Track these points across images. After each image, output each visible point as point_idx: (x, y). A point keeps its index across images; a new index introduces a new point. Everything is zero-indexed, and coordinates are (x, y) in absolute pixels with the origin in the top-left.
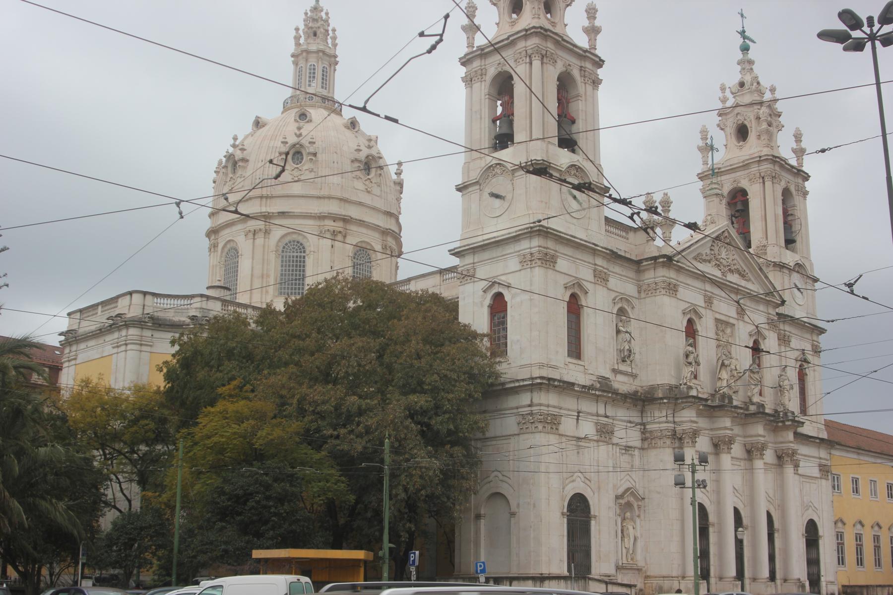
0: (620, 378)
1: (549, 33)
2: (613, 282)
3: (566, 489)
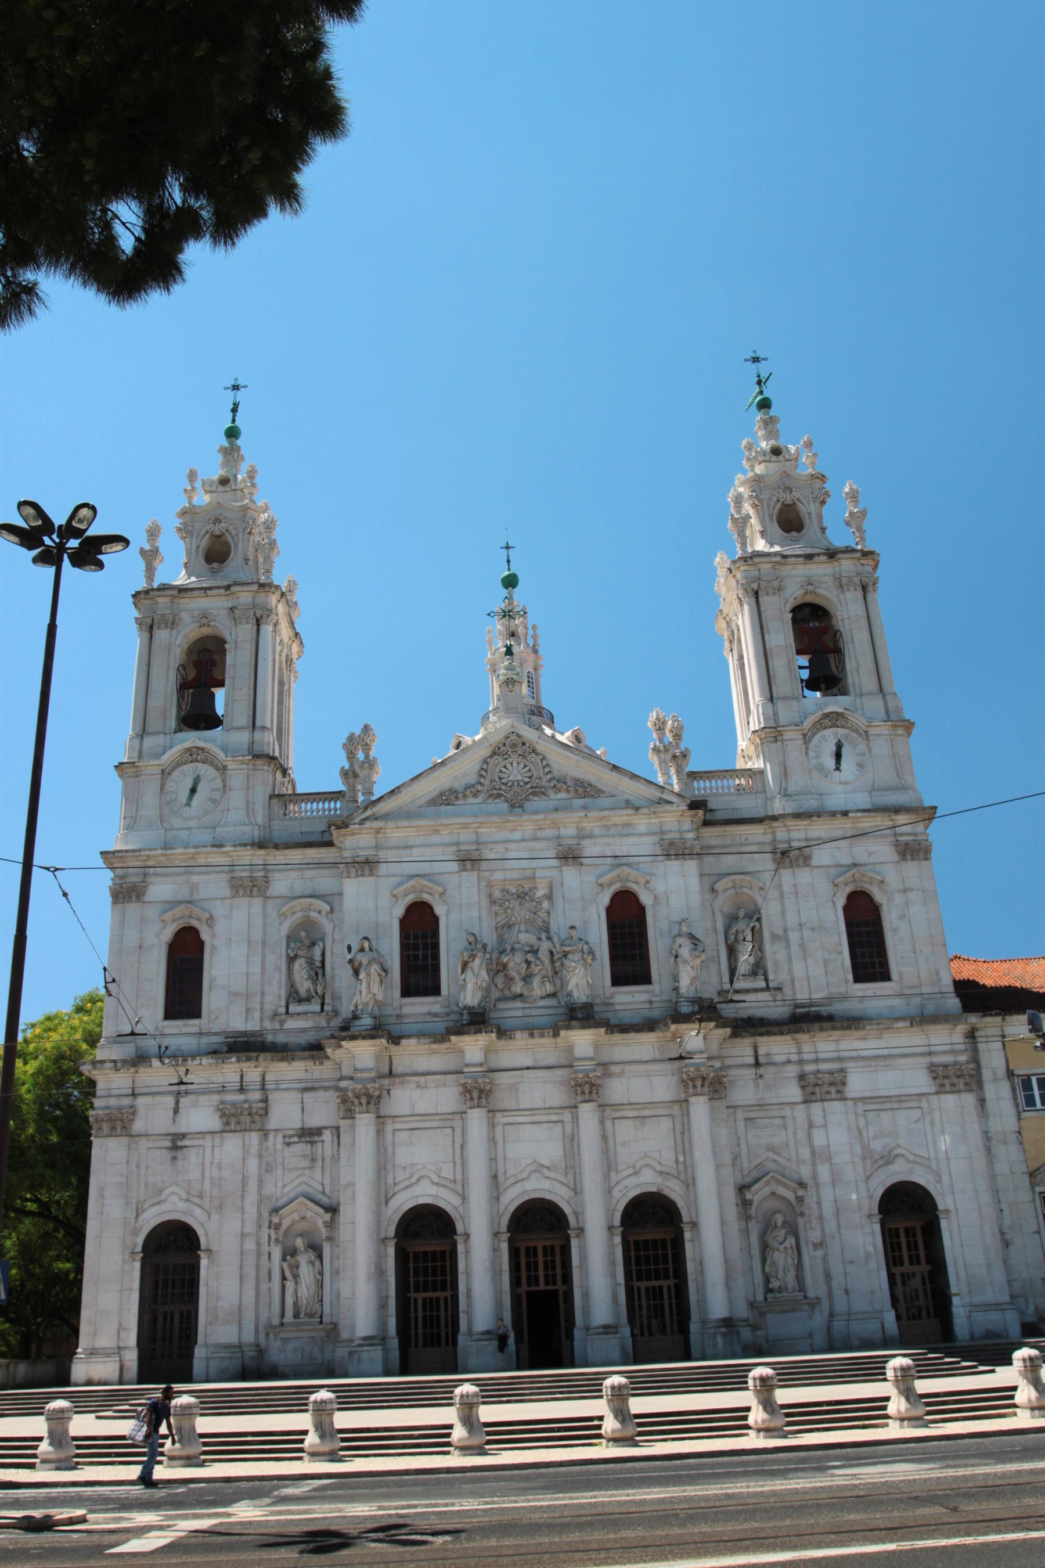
0: (291, 1024)
3: (143, 1216)
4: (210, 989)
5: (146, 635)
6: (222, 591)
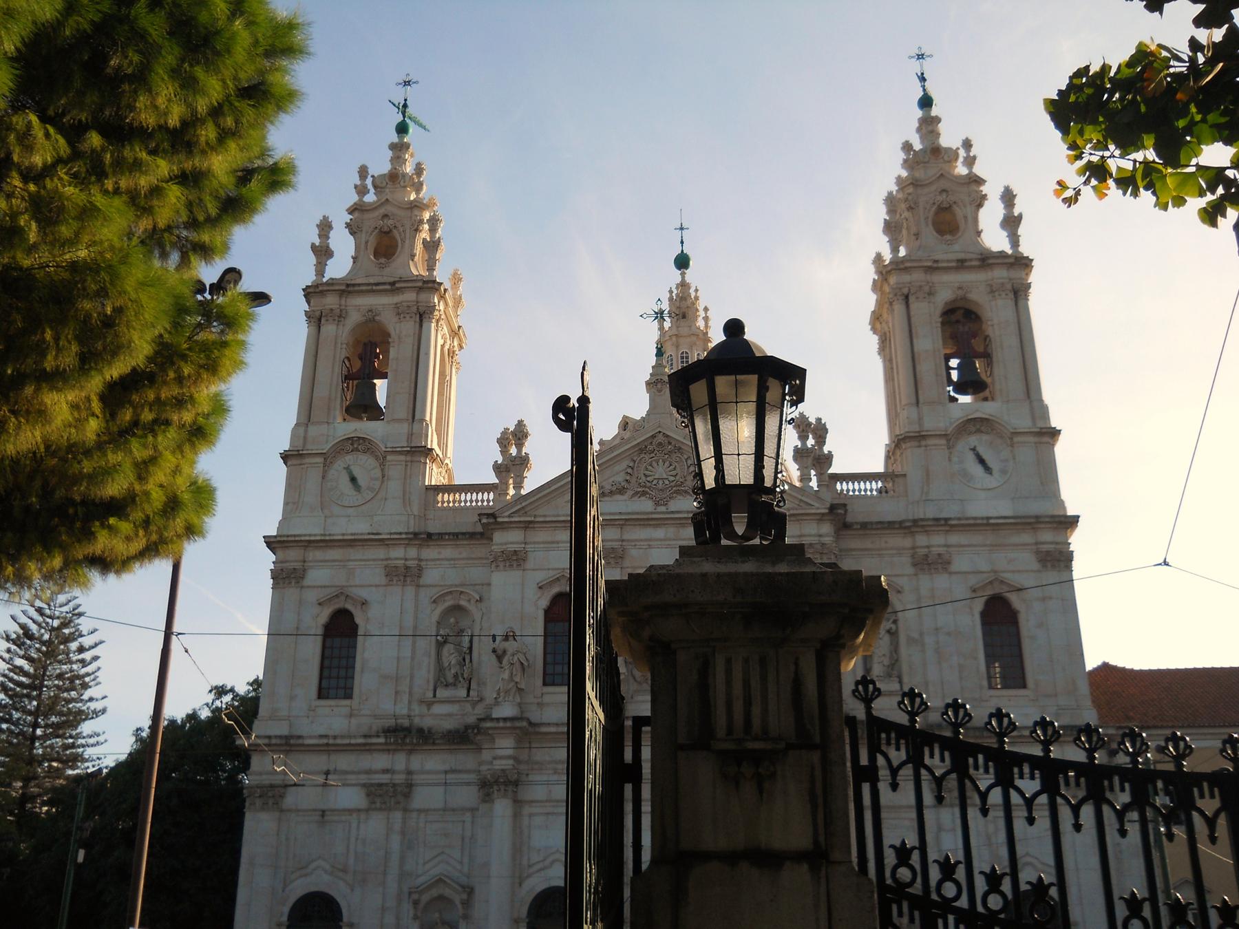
0: (438, 709)
1: (320, 288)
2: (432, 576)
4: (362, 671)
5: (314, 329)
6: (388, 287)
